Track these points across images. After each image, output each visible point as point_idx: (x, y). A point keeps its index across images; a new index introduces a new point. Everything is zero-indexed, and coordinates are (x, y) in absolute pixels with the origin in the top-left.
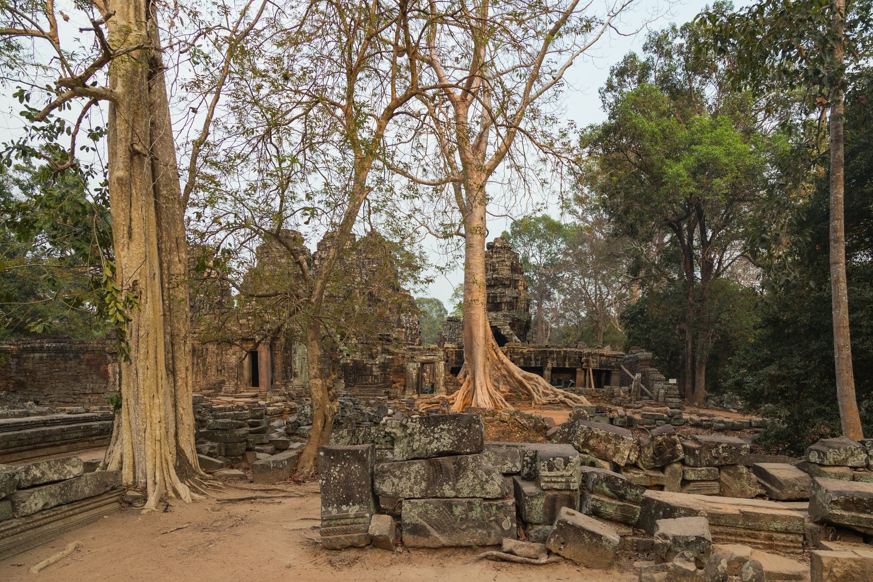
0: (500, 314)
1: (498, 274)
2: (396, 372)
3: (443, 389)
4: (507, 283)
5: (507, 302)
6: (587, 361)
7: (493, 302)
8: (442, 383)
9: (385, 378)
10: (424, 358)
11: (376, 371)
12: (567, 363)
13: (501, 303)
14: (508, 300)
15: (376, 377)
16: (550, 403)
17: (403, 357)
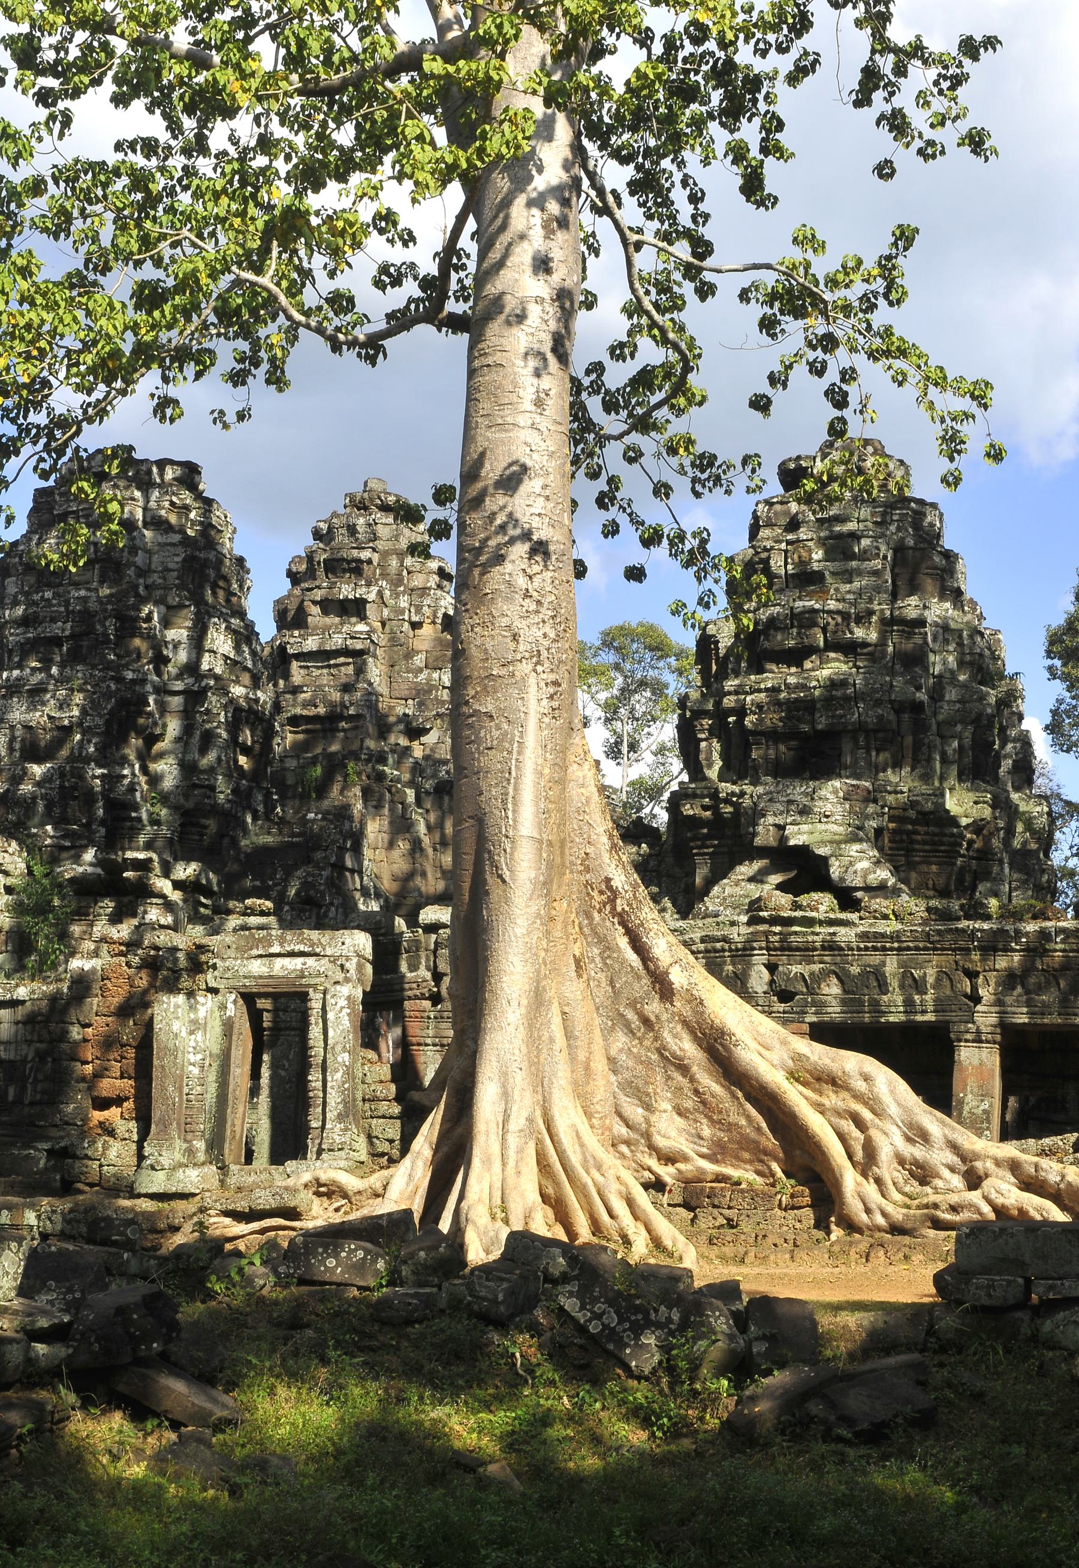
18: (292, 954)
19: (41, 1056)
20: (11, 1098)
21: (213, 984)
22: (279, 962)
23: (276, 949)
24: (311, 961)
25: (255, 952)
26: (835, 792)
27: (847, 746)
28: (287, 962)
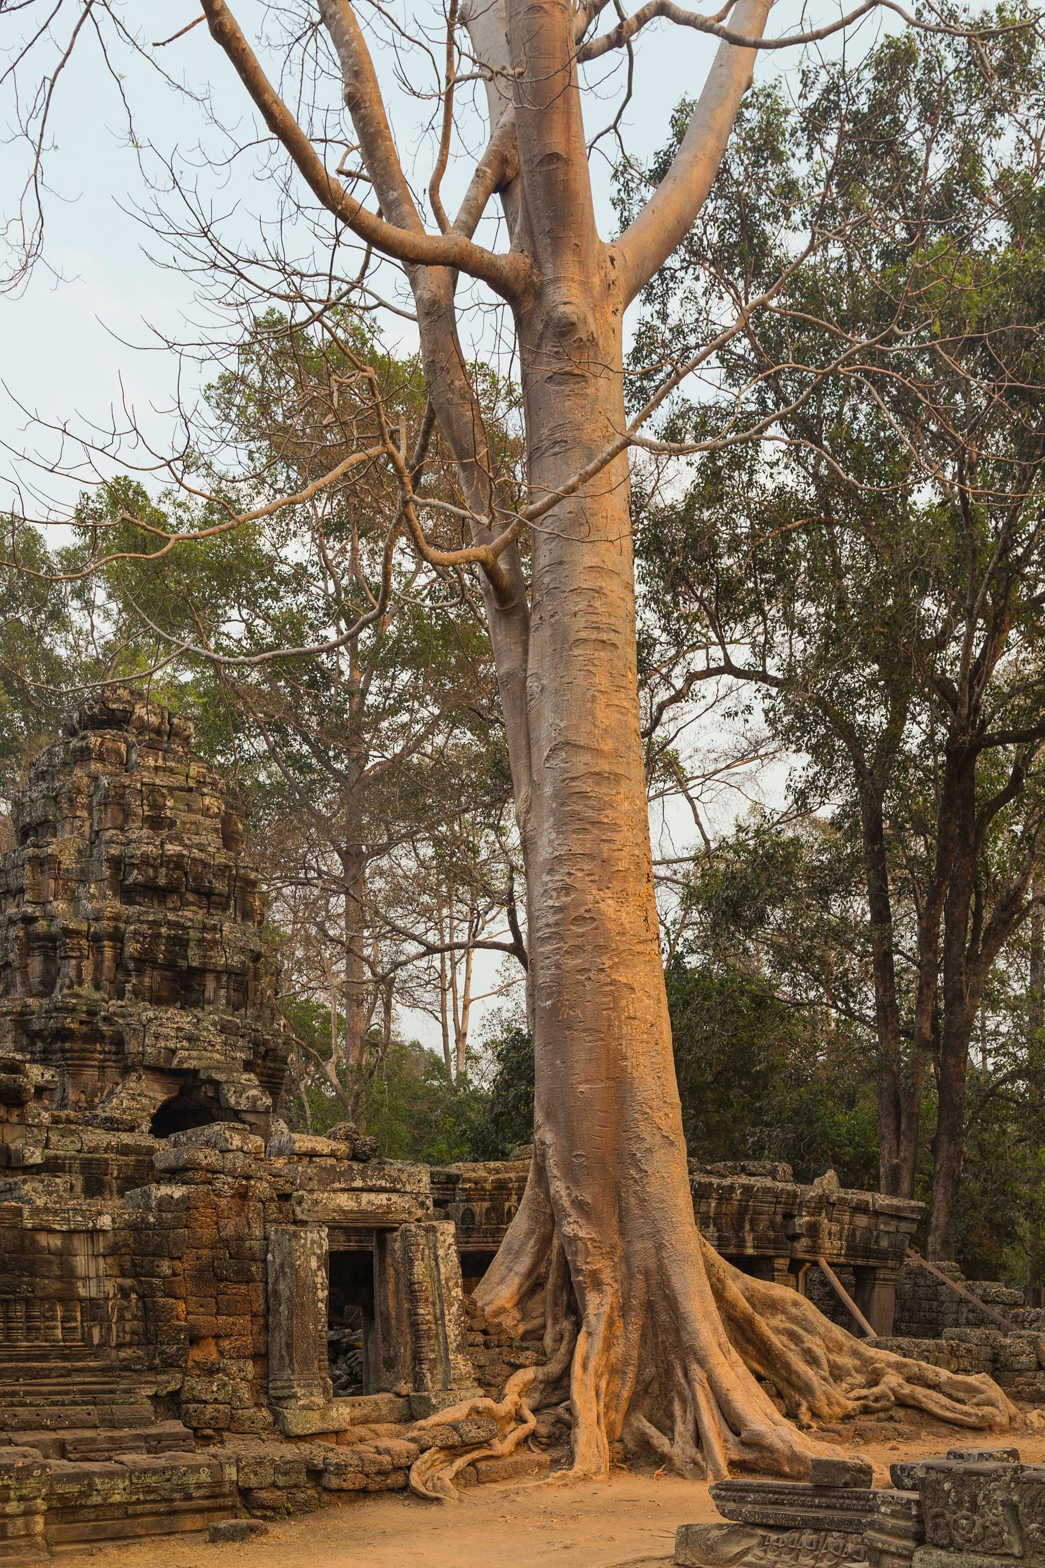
0: (210, 1018)
1: (178, 839)
2: (210, 1277)
3: (461, 1364)
4: (220, 886)
5: (229, 971)
6: (813, 1230)
7: (170, 965)
8: (452, 1331)
9: (149, 1312)
10: (345, 1201)
11: (94, 1275)
12: (749, 1238)
13: (201, 972)
14: (236, 960)
15: (93, 1308)
16: (866, 1410)
17: (242, 1195)
18: (370, 1190)
19: (124, 1292)
20: (96, 1341)
21: (300, 1216)
22: (365, 1197)
23: (358, 1183)
24: (394, 1197)
25: (337, 1185)
26: (214, 1024)
27: (210, 984)
28: (372, 1196)
